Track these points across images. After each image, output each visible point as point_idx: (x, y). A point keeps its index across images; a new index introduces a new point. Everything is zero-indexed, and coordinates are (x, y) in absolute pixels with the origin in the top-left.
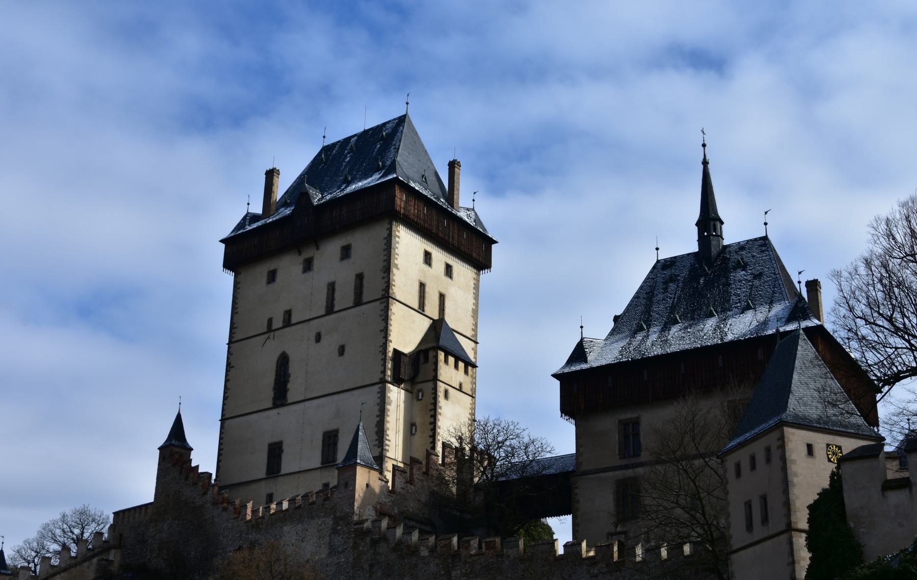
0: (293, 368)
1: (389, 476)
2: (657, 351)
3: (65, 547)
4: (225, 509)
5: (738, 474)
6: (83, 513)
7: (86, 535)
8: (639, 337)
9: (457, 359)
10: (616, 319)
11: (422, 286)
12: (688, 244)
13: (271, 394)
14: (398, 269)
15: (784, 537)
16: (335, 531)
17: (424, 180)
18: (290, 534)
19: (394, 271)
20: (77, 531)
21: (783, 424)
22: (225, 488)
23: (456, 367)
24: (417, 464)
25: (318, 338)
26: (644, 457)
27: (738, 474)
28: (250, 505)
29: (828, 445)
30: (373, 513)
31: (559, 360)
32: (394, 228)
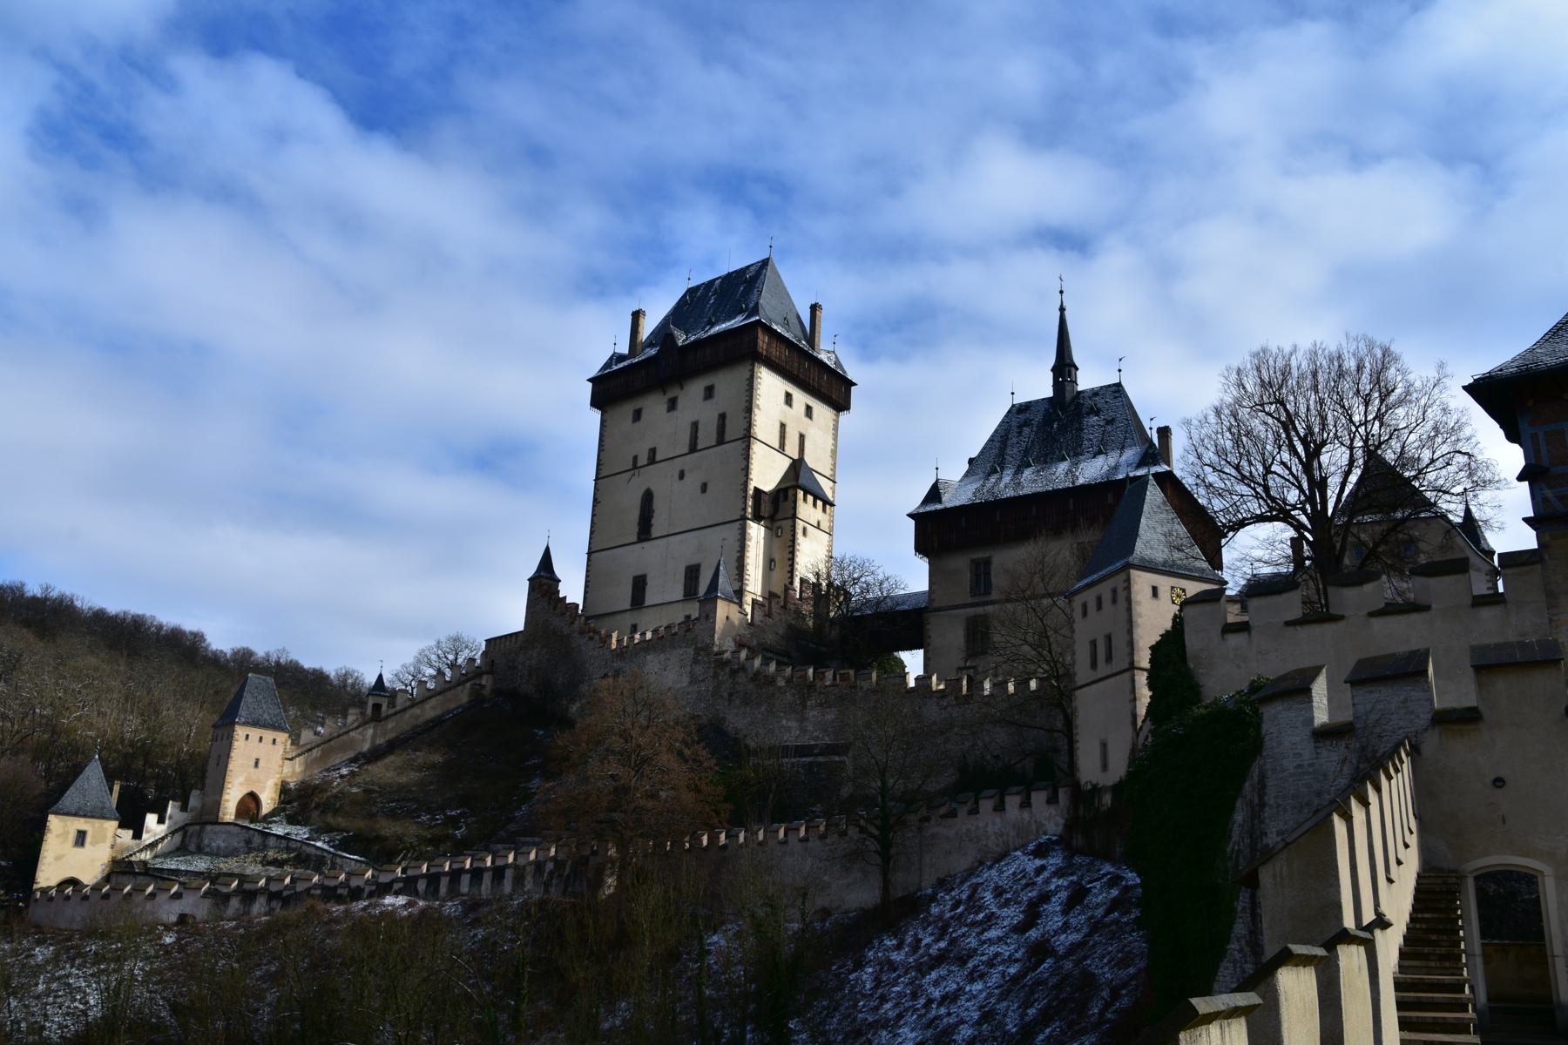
0: (658, 504)
1: (748, 609)
2: (1010, 493)
3: (440, 672)
4: (591, 639)
5: (1085, 614)
6: (456, 639)
7: (460, 661)
8: (993, 479)
9: (816, 498)
10: (971, 461)
12: (1041, 387)
15: (1127, 675)
16: (695, 661)
17: (786, 323)
18: (653, 662)
19: (756, 411)
20: (451, 657)
21: (1129, 566)
22: (590, 620)
23: (815, 505)
24: (774, 599)
25: (682, 475)
26: (994, 595)
27: (1085, 614)
28: (615, 635)
30: (732, 644)
31: (915, 500)
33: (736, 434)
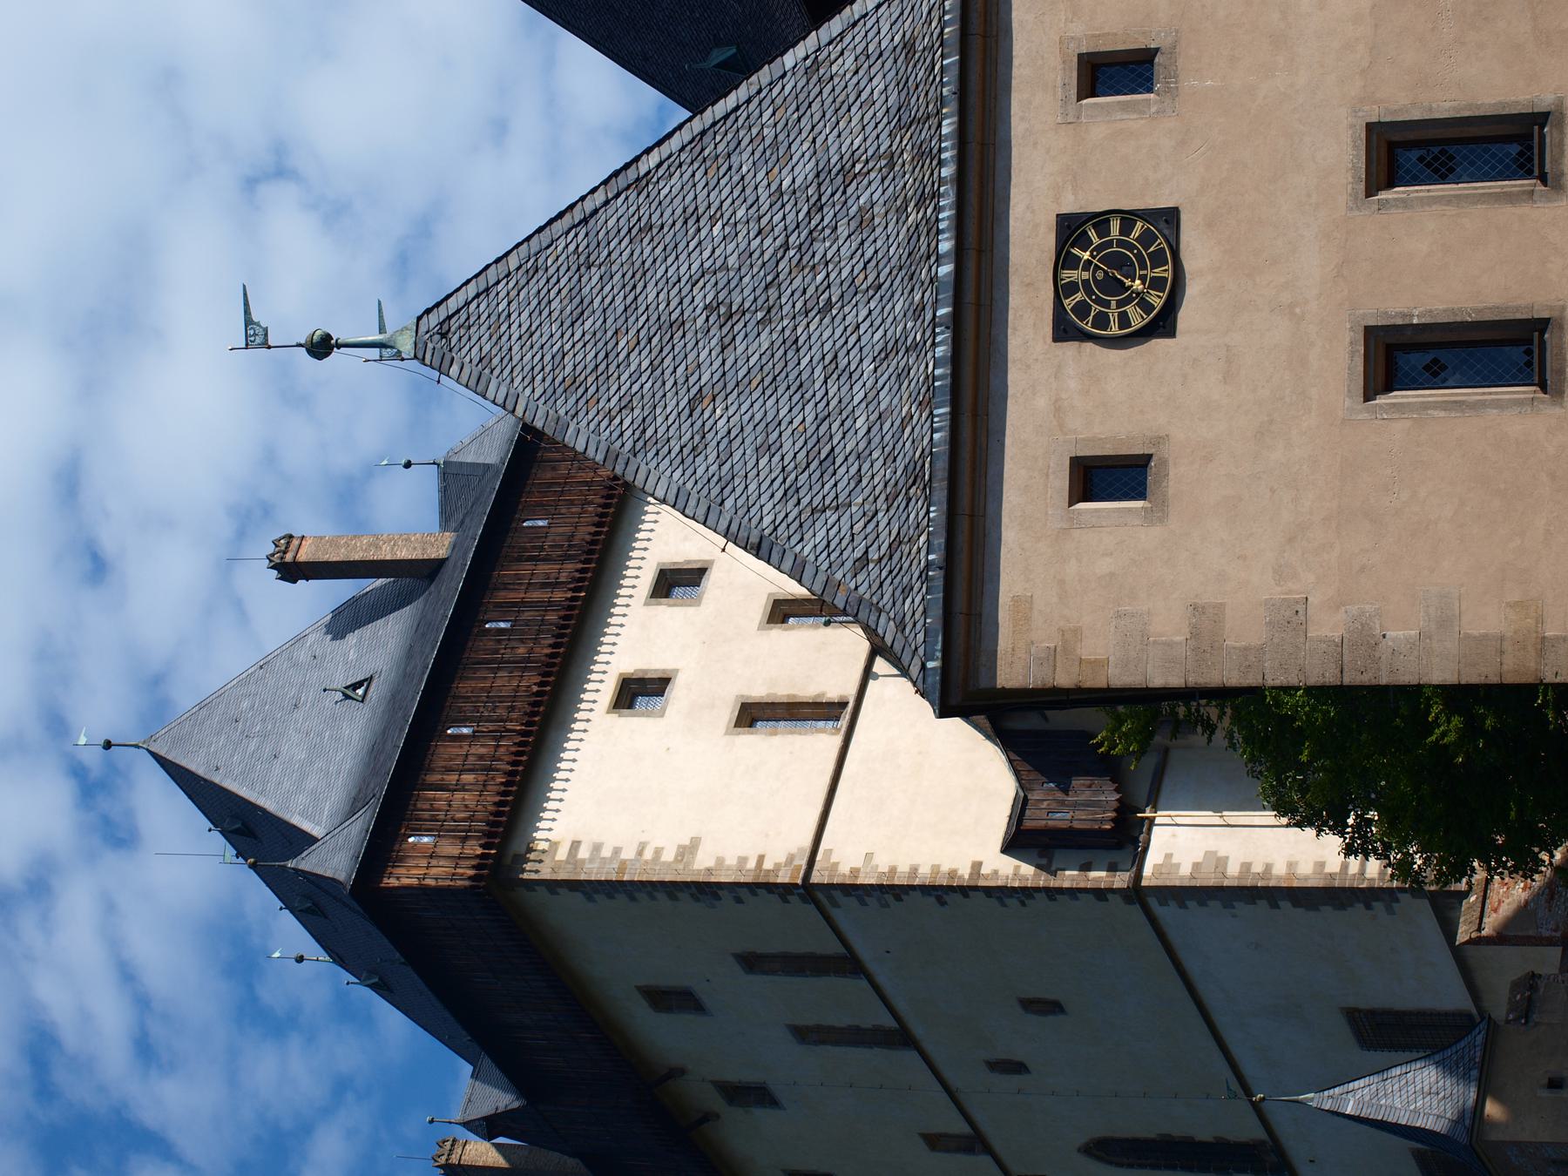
11: (751, 715)
14: (695, 844)
19: (702, 865)
32: (546, 873)
33: (810, 927)
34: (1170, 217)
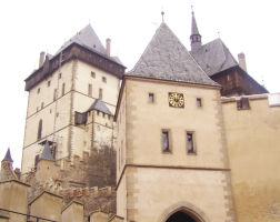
13: (36, 136)
29: (170, 94)
34: (183, 107)
